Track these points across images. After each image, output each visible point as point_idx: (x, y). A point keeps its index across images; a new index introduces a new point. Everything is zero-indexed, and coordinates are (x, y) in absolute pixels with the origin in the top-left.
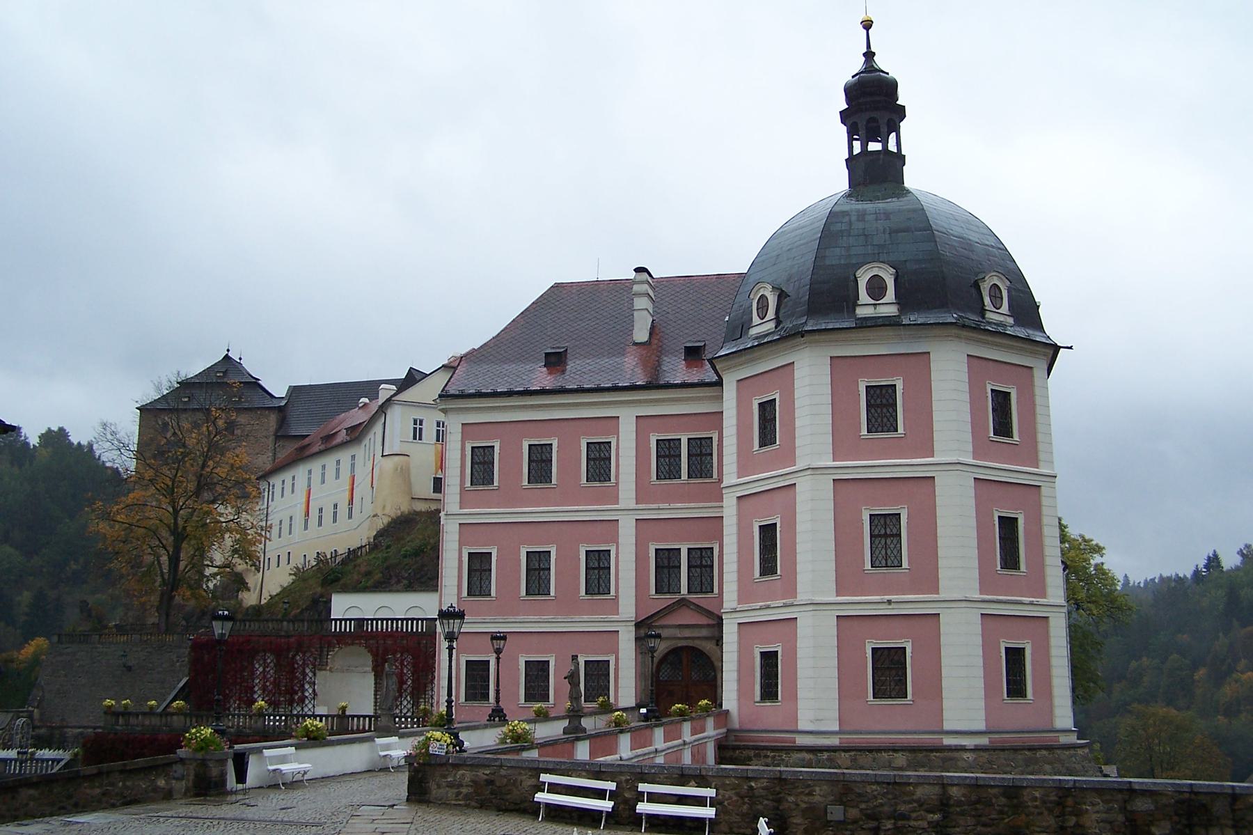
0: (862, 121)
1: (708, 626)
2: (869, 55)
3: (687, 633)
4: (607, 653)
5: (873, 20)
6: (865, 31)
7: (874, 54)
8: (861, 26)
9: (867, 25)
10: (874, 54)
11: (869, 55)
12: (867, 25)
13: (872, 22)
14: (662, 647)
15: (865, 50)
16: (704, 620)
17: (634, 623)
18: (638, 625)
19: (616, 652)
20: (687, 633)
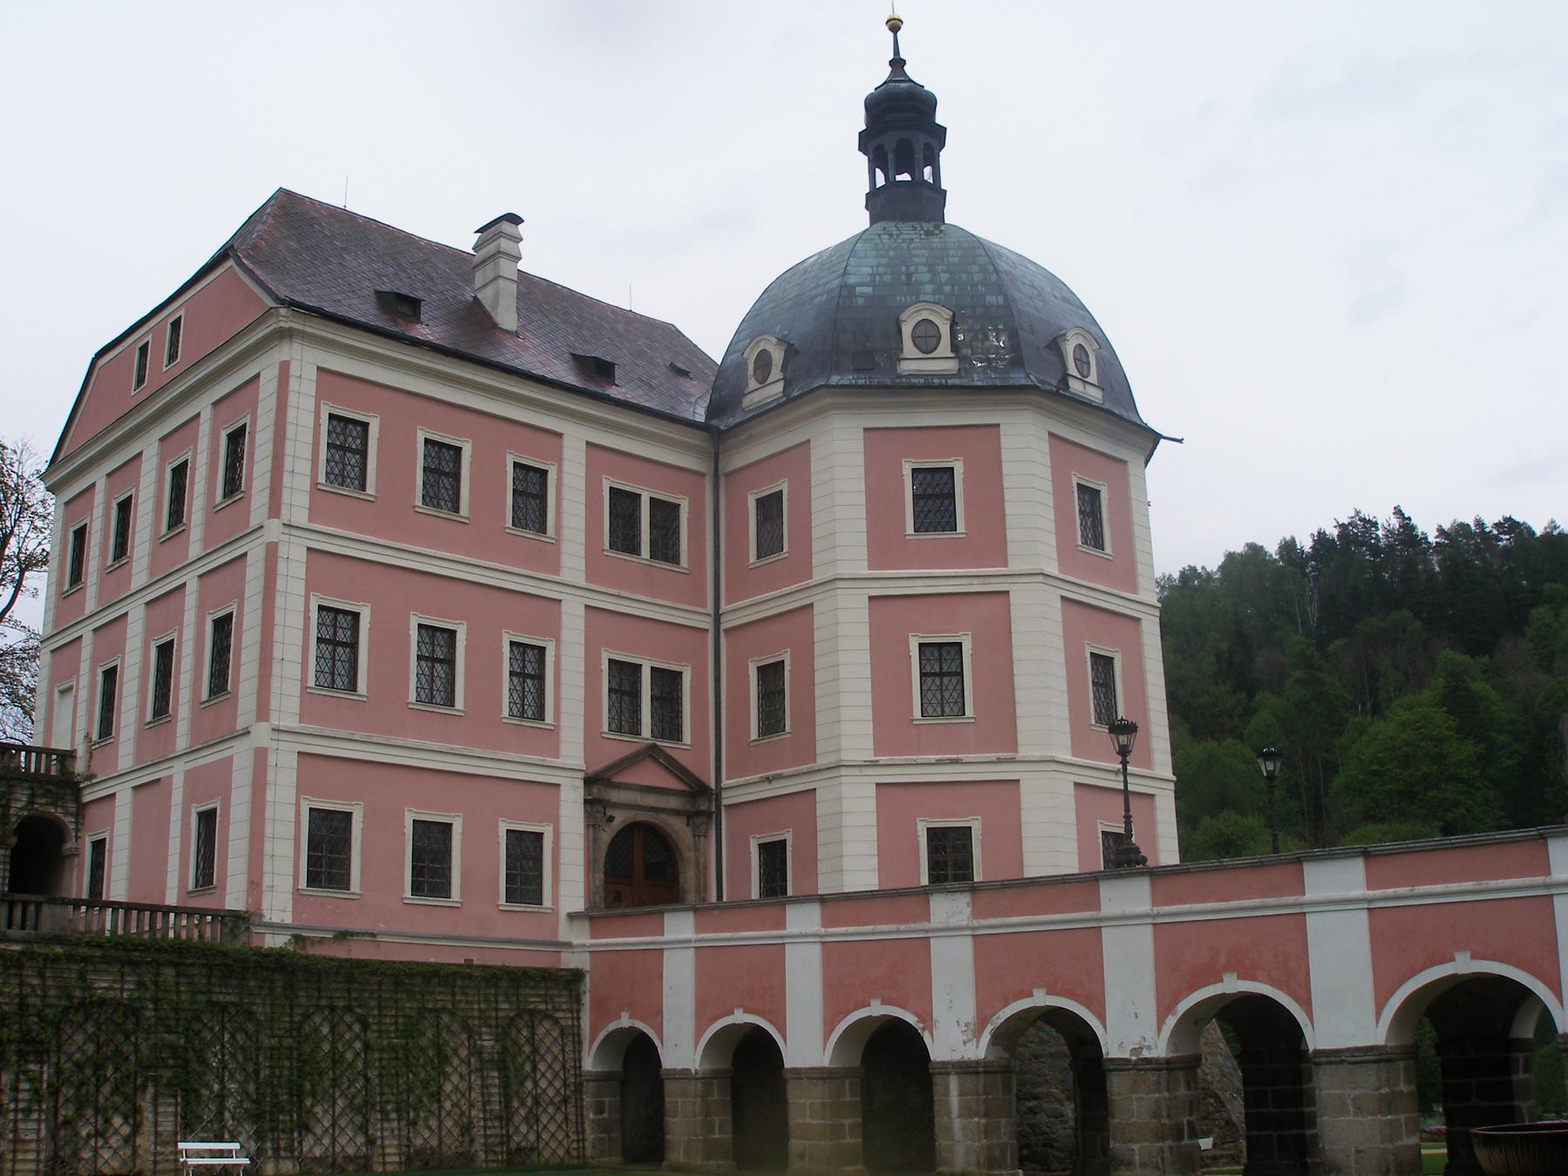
0: (890, 141)
1: (681, 793)
2: (897, 63)
3: (651, 800)
4: (540, 821)
5: (902, 19)
6: (891, 34)
7: (904, 62)
8: (886, 28)
9: (895, 26)
10: (904, 62)
11: (897, 63)
12: (895, 26)
13: (902, 22)
14: (621, 818)
15: (891, 57)
16: (679, 786)
17: (582, 775)
18: (589, 781)
19: (555, 820)
20: (651, 800)
